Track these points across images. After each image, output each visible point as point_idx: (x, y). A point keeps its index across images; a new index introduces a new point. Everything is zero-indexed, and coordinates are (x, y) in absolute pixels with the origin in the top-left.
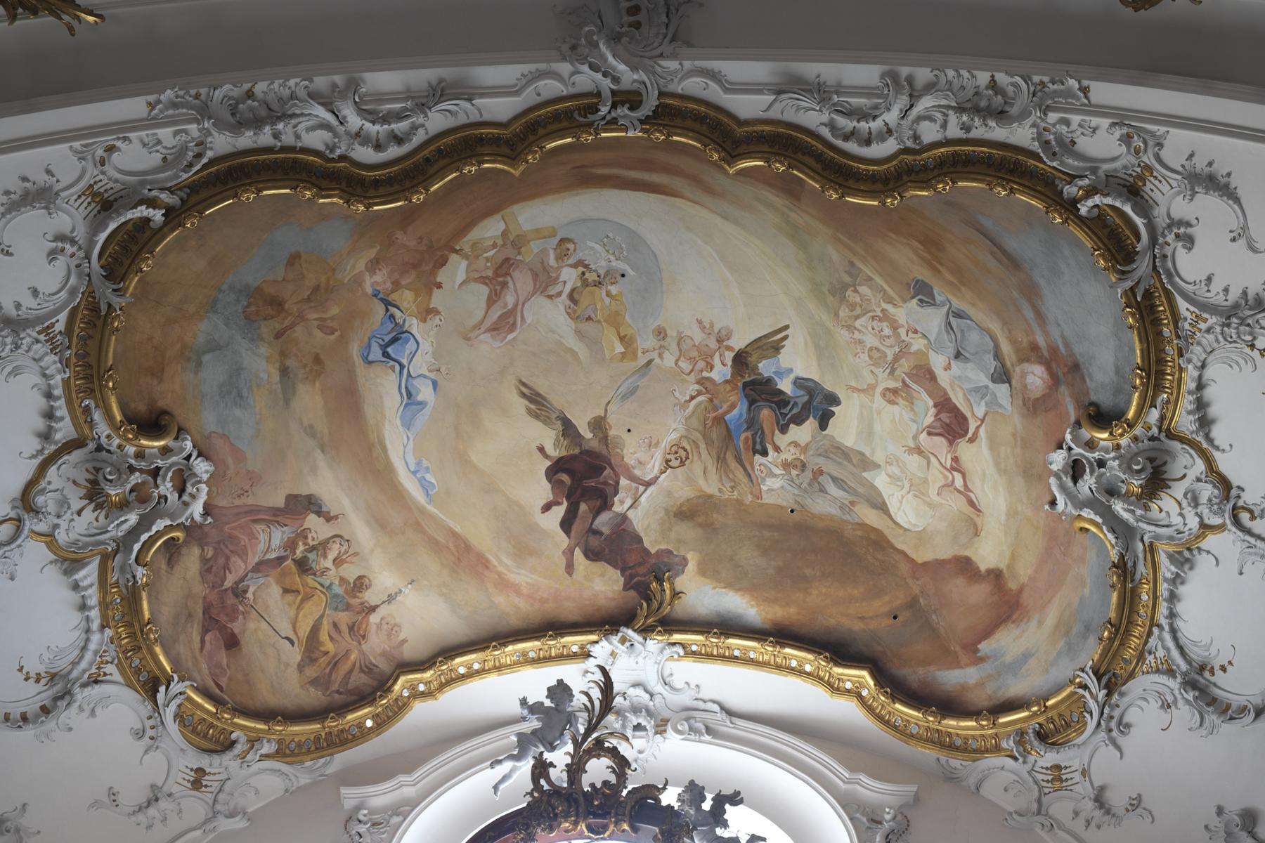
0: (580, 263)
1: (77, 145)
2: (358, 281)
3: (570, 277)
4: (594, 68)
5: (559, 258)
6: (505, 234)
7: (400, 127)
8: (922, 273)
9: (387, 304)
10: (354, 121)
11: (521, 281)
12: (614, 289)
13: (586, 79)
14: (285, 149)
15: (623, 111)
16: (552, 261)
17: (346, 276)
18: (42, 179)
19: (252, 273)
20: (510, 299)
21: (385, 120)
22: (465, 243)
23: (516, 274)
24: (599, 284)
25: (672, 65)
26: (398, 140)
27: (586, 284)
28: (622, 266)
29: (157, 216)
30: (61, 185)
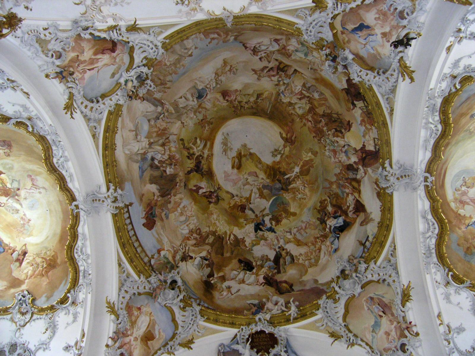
0: (461, 186)
1: (436, 288)
2: (463, 232)
3: (464, 188)
4: (419, 186)
5: (459, 191)
6: (454, 202)
7: (431, 224)
8: (468, 117)
9: (468, 225)
10: (430, 234)
11: (464, 198)
12: (467, 179)
13: (422, 188)
14: (436, 247)
15: (428, 180)
16: (460, 192)
17: (462, 234)
18: (443, 296)
19: (461, 253)
20: (468, 200)
21: (430, 227)
22: (455, 210)
23: (463, 199)
24: (466, 182)
25: (419, 170)
26: (434, 224)
27: (466, 185)
28: (462, 178)
29: (450, 273)
30: (444, 291)
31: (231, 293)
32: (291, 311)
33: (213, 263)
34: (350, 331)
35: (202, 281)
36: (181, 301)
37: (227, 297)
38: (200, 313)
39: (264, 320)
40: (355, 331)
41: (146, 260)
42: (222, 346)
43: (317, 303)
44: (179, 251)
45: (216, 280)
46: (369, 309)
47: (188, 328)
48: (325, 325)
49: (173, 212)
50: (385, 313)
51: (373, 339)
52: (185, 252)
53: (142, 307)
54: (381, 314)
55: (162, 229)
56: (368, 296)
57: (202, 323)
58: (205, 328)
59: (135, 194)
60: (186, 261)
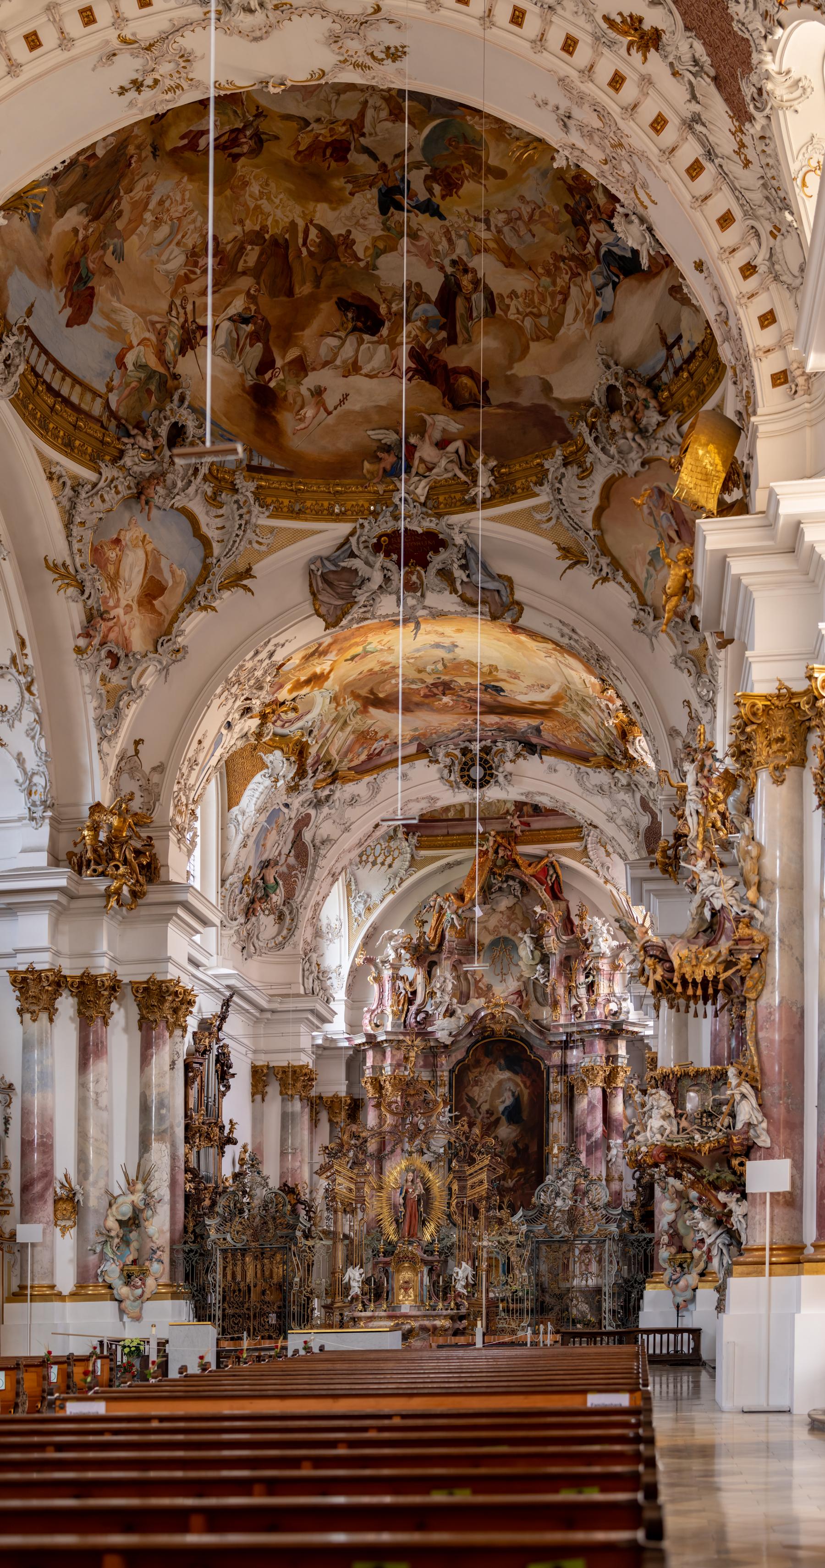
31: (326, 410)
32: (477, 489)
33: (267, 327)
34: (605, 551)
35: (244, 389)
36: (205, 479)
37: (316, 421)
38: (257, 499)
39: (414, 501)
40: (615, 553)
41: (97, 409)
42: (318, 563)
43: (542, 466)
44: (171, 328)
45: (281, 376)
46: (651, 513)
47: (233, 546)
48: (553, 521)
49: (133, 231)
50: (679, 537)
51: (647, 579)
52: (186, 321)
53: (123, 533)
54: (673, 535)
55: (113, 294)
56: (655, 484)
57: (264, 521)
58: (272, 530)
59: (32, 277)
60: (193, 348)
